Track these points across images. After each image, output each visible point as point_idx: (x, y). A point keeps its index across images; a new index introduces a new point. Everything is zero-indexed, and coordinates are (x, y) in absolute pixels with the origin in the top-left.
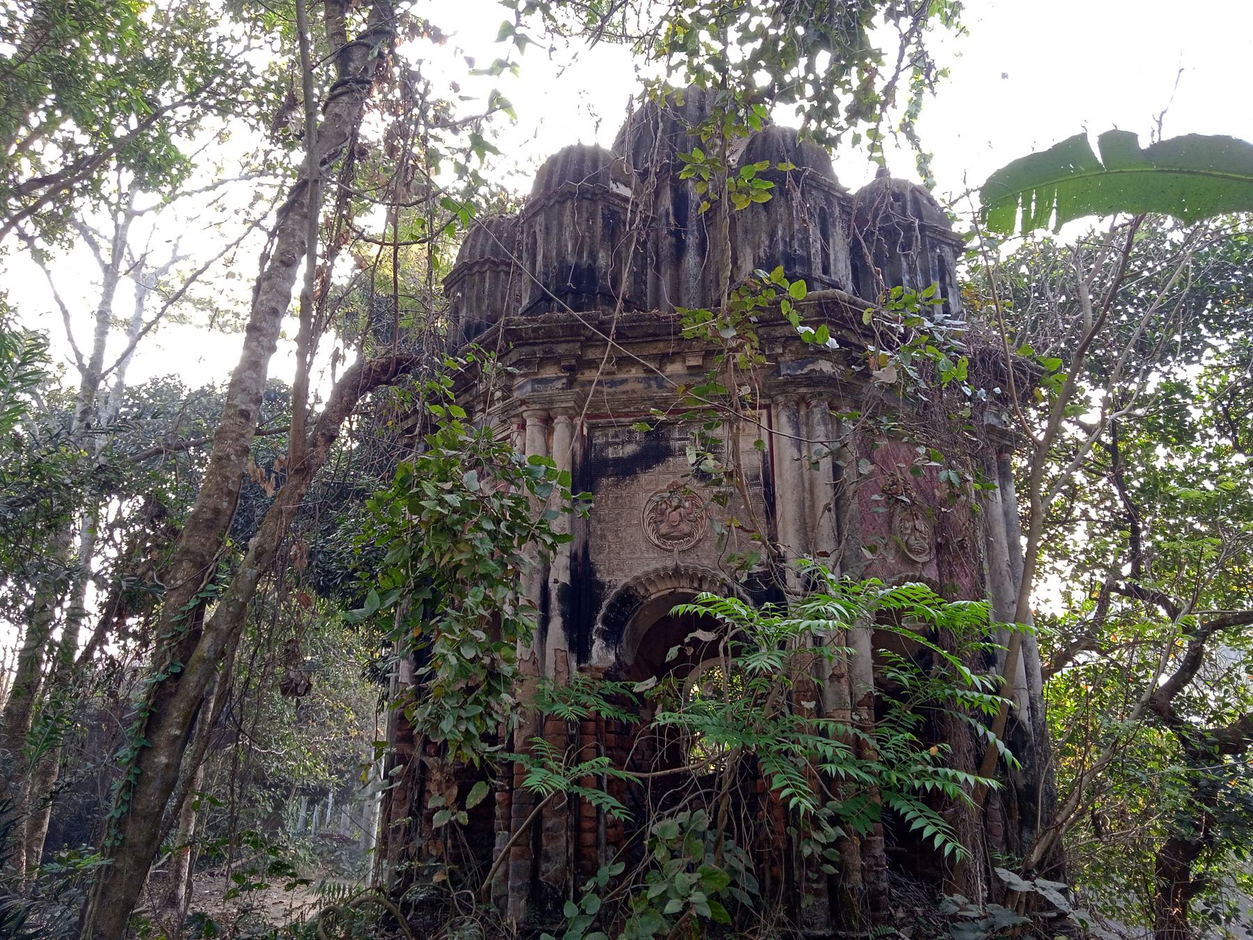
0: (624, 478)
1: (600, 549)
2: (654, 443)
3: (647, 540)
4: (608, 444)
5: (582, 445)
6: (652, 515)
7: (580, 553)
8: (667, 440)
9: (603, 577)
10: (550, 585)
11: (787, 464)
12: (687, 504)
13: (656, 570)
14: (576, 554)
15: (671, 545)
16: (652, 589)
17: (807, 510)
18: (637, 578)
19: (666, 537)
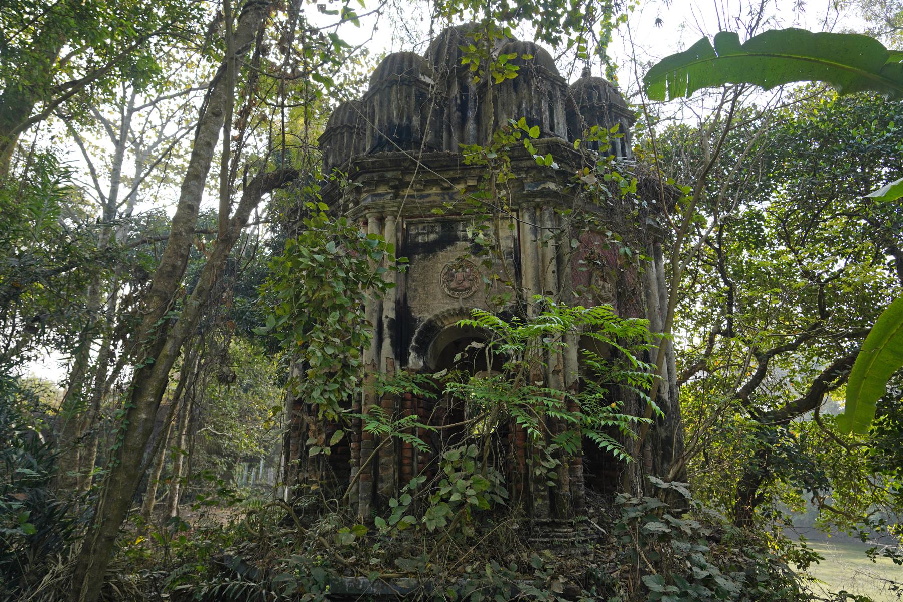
1: (414, 298)
3: (443, 292)
4: (419, 234)
7: (402, 300)
8: (456, 231)
9: (416, 314)
11: (528, 245)
12: (467, 270)
13: (448, 311)
16: (446, 322)
18: (437, 315)
19: (454, 290)
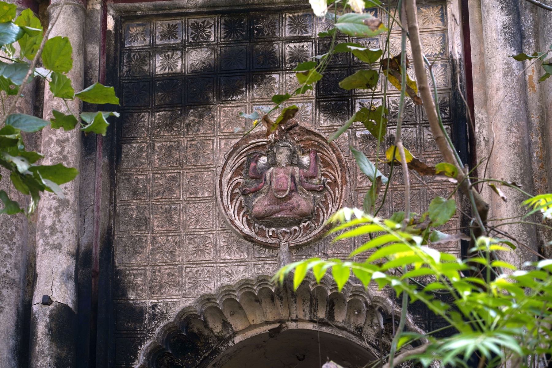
0: (185, 113)
1: (137, 245)
2: (244, 47)
3: (229, 227)
4: (154, 50)
5: (104, 51)
6: (239, 179)
7: (96, 251)
8: (270, 41)
9: (141, 297)
10: (35, 308)
11: (497, 78)
12: (306, 160)
13: (245, 285)
14: (88, 253)
15: (275, 236)
16: (237, 324)
17: (536, 166)
18: (207, 299)
19: (262, 220)
